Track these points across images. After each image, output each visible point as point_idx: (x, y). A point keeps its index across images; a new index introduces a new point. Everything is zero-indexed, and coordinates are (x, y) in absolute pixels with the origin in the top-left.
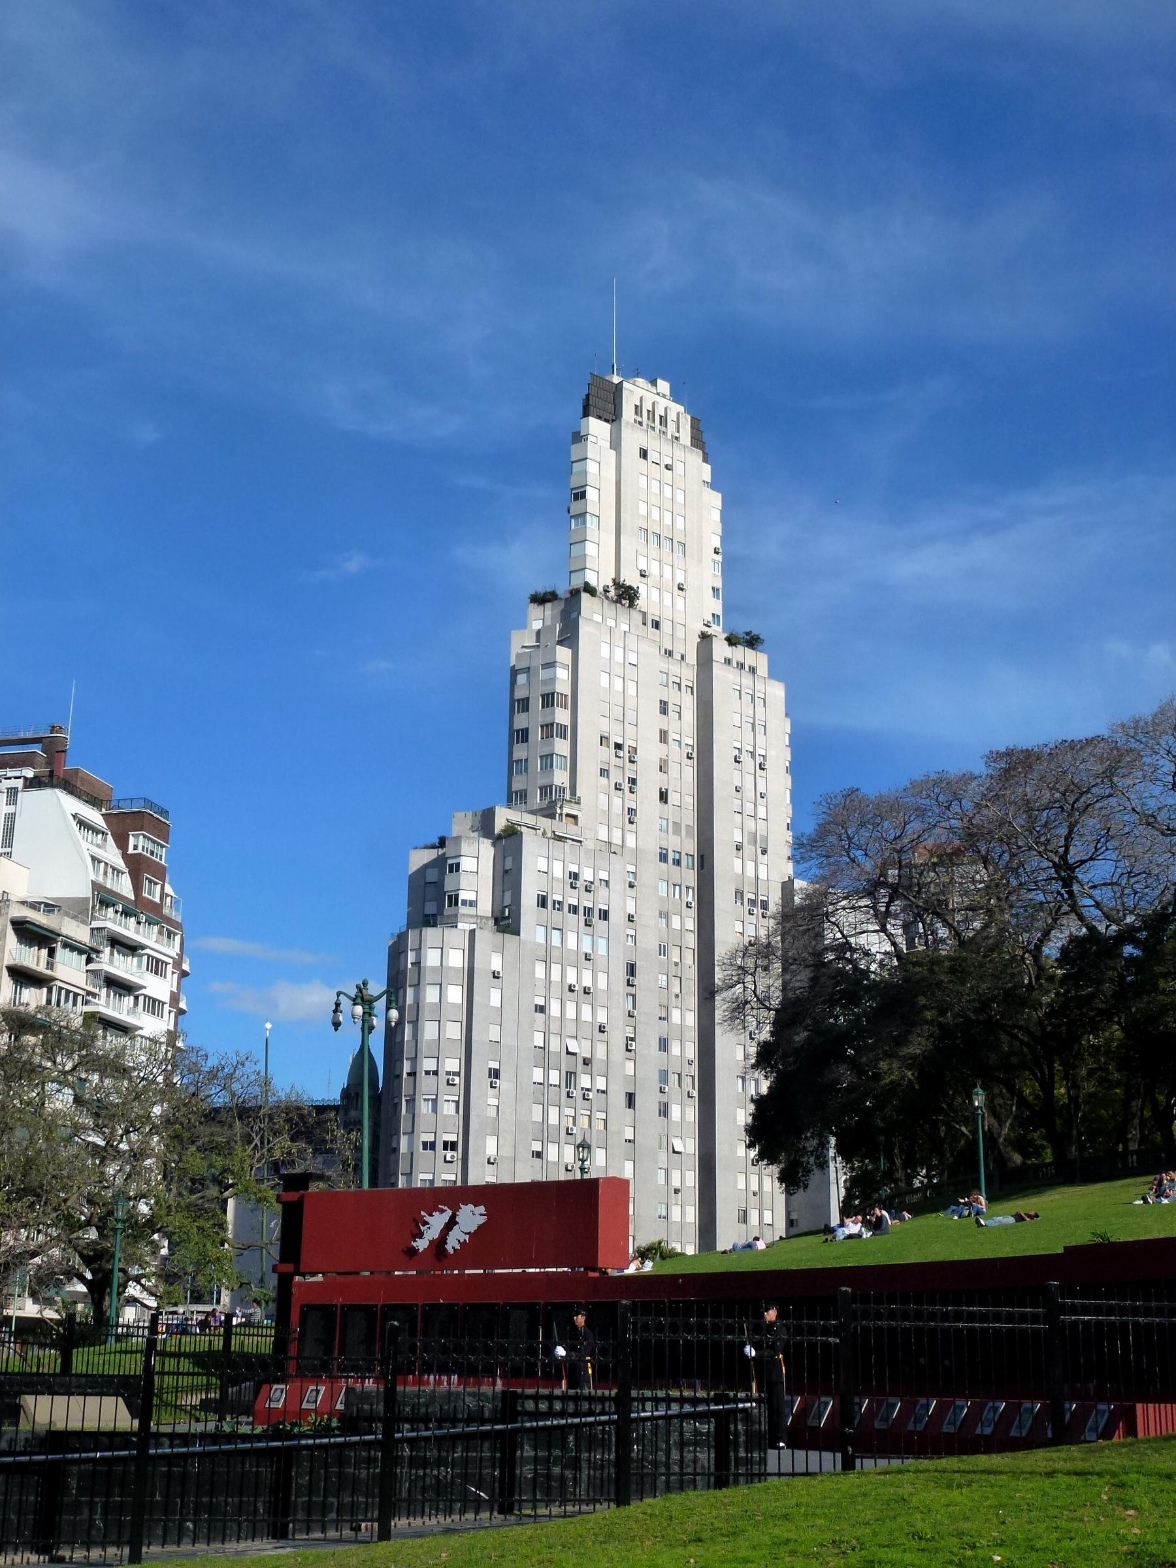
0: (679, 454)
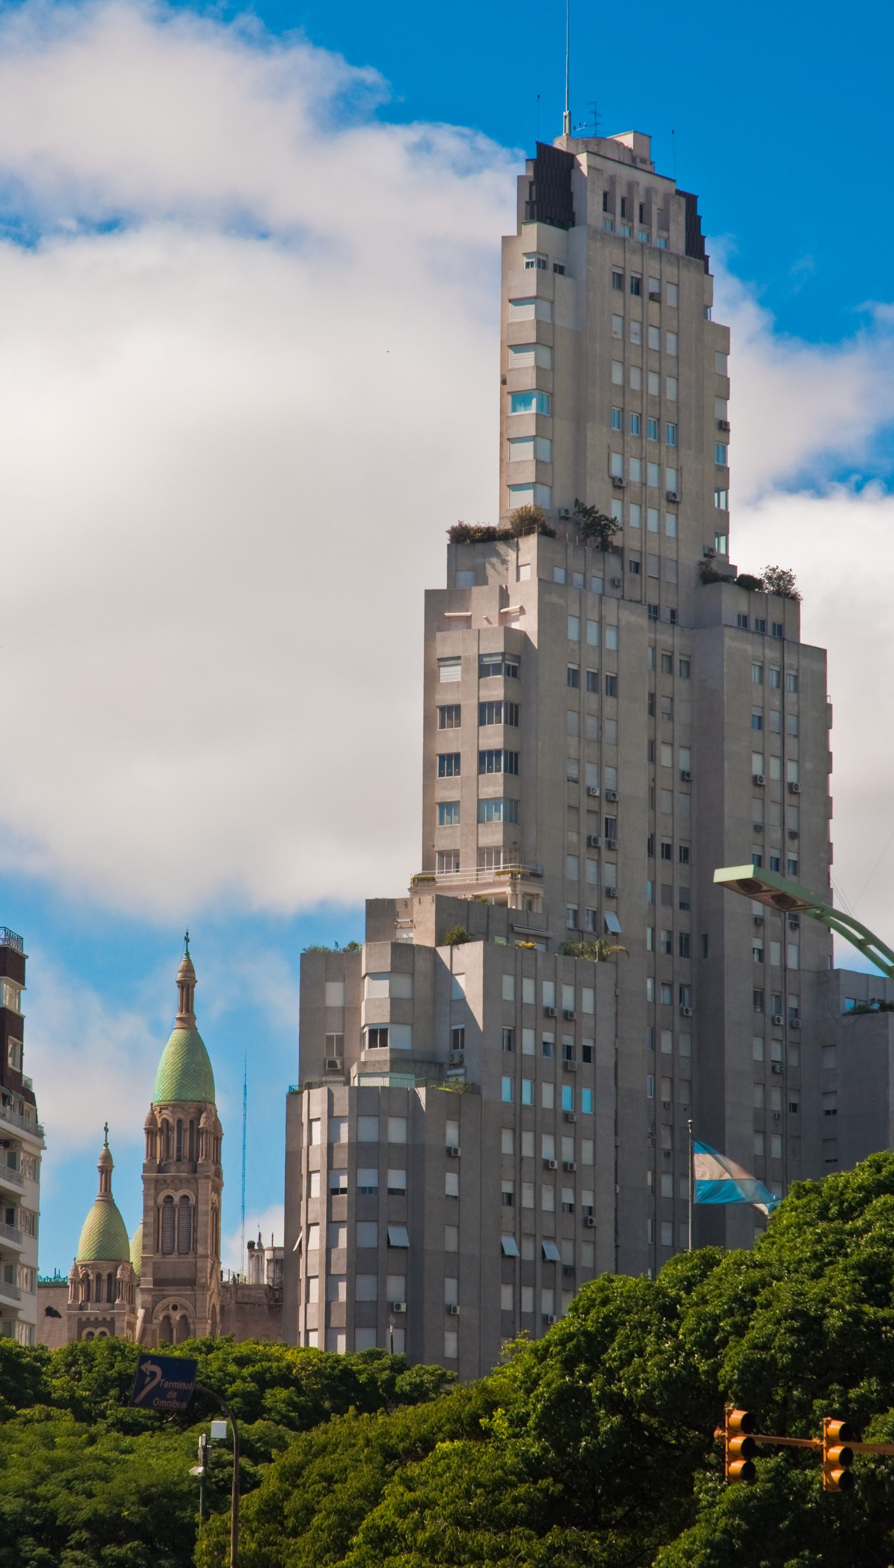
0: (670, 272)
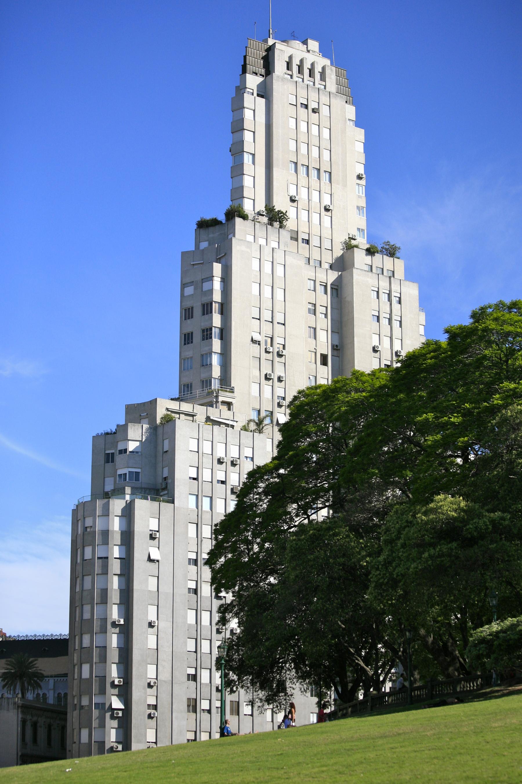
0: (325, 99)
